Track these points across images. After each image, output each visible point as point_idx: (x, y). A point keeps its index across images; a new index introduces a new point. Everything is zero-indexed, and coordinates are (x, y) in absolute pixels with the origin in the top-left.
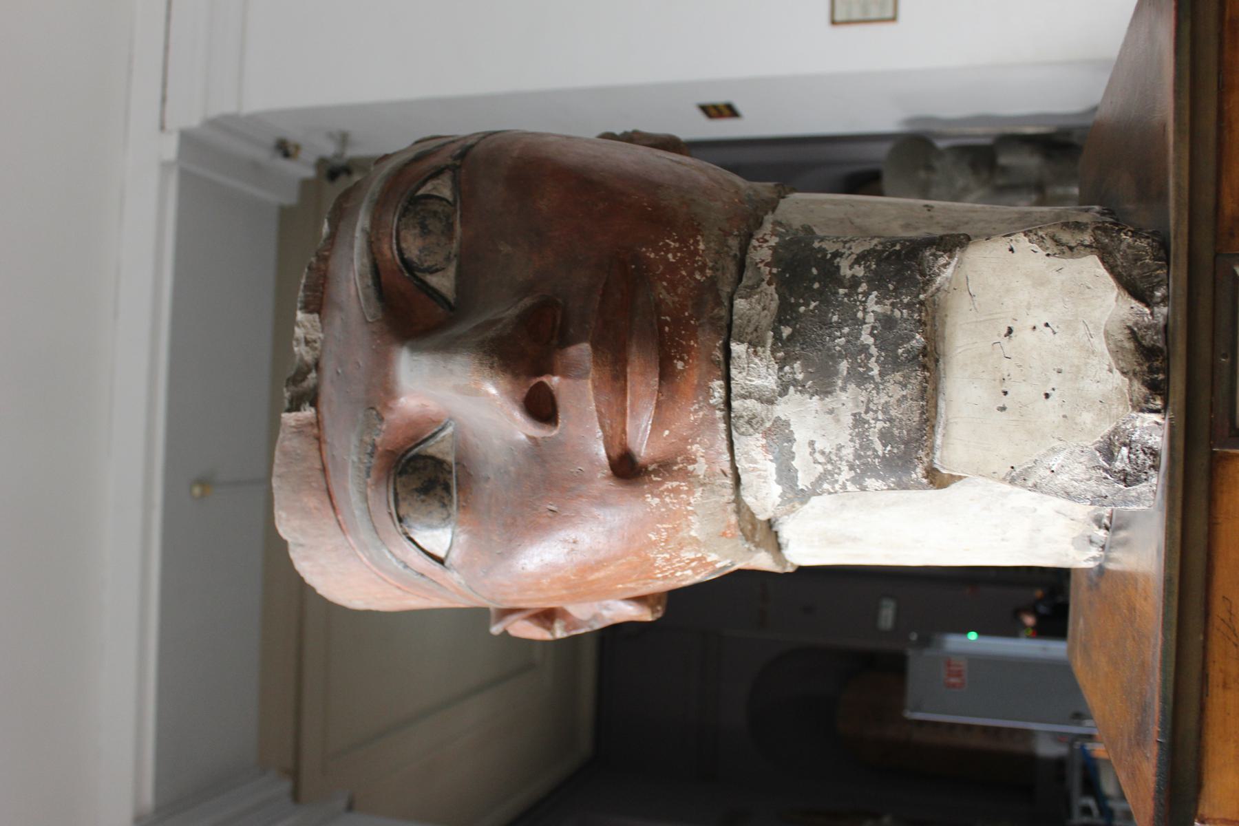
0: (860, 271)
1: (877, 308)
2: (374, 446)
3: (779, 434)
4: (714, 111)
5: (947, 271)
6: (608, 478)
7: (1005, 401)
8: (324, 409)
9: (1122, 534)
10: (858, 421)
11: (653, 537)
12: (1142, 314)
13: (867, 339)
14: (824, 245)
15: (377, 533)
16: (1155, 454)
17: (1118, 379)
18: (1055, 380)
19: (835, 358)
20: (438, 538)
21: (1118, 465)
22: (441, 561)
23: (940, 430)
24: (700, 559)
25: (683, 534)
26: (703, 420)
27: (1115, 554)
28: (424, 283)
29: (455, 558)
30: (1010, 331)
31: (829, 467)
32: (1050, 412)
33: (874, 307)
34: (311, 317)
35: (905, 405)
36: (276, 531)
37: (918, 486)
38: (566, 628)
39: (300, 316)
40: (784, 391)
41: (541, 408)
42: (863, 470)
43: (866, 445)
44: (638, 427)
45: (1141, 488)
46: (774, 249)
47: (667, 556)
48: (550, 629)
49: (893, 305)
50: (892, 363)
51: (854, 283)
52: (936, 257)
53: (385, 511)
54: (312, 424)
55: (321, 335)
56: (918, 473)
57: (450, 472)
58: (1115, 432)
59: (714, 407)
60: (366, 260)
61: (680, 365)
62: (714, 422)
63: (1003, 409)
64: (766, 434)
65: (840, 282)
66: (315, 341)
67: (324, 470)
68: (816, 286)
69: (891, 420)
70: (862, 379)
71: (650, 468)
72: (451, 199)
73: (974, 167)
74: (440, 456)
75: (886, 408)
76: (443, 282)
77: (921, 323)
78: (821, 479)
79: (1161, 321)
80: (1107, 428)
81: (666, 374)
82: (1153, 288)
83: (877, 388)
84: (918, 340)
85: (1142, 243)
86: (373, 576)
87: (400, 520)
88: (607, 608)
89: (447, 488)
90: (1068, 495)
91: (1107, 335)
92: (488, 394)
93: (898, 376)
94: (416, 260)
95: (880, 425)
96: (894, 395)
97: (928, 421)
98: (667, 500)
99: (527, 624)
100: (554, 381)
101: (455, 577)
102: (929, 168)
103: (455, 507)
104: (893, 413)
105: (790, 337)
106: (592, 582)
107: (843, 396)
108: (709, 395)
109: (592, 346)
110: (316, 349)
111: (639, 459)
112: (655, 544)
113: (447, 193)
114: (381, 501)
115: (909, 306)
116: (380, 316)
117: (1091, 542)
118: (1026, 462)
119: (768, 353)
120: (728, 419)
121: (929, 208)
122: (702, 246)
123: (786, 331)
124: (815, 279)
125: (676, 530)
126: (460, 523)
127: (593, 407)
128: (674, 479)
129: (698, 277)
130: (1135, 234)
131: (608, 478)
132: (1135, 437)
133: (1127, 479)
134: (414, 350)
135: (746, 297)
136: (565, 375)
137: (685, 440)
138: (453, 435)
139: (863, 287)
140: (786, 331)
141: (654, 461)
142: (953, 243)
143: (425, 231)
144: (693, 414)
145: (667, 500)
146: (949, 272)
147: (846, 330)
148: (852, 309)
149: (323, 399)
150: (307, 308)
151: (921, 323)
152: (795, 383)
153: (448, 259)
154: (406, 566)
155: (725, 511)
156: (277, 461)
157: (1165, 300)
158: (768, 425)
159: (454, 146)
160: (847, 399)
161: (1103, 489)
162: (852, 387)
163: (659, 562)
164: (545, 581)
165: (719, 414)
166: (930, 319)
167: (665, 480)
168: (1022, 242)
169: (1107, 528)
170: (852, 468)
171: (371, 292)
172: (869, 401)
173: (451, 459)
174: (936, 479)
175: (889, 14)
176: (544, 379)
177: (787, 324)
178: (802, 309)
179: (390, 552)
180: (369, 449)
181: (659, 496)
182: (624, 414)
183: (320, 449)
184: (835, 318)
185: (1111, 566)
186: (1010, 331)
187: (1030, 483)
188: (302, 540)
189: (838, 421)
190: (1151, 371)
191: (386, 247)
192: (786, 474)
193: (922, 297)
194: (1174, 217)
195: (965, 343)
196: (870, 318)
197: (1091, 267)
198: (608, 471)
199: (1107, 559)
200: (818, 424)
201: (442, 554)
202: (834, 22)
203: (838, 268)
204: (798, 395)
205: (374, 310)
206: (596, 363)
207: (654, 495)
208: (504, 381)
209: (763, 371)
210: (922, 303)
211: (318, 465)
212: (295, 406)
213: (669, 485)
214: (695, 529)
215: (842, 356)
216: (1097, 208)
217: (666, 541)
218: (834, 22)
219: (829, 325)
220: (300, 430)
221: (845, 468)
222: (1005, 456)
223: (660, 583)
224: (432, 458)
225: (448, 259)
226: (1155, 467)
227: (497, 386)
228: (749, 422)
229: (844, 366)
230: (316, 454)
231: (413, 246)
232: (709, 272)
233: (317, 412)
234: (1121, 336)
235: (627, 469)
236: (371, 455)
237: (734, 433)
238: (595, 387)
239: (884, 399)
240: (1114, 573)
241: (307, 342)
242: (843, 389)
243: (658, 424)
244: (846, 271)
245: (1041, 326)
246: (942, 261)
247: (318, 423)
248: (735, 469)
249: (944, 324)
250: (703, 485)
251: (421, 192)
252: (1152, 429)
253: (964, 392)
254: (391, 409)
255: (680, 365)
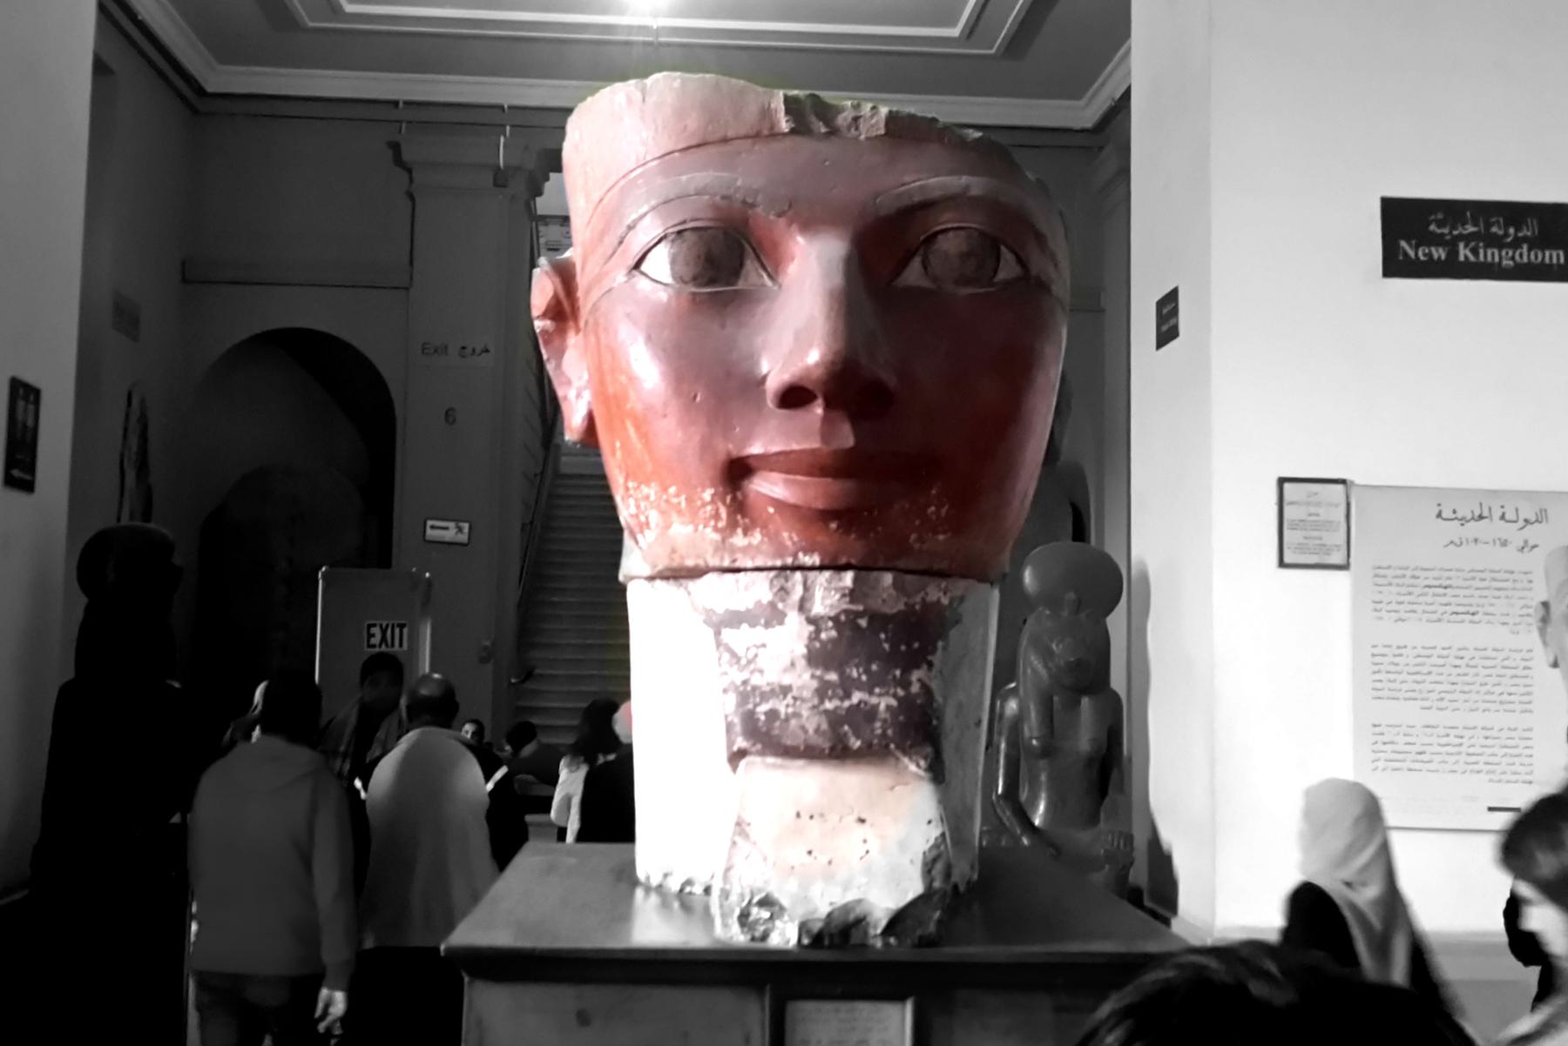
0: (915, 688)
1: (882, 707)
2: (753, 206)
3: (773, 616)
4: (1168, 307)
5: (913, 767)
6: (729, 454)
7: (805, 817)
8: (788, 143)
9: (676, 905)
10: (785, 690)
11: (672, 490)
12: (875, 927)
13: (857, 697)
14: (939, 652)
15: (665, 202)
16: (765, 937)
17: (823, 910)
18: (824, 859)
19: (840, 668)
20: (660, 264)
21: (755, 910)
22: (637, 266)
23: (778, 761)
24: (647, 524)
25: (675, 517)
26: (786, 547)
27: (654, 899)
28: (913, 254)
29: (642, 284)
30: (862, 821)
31: (743, 662)
32: (796, 856)
33: (884, 702)
34: (882, 125)
35: (800, 733)
36: (660, 70)
37: (730, 743)
38: (544, 332)
39: (884, 111)
40: (810, 621)
41: (794, 397)
42: (746, 694)
43: (765, 697)
44: (775, 484)
45: (735, 928)
46: (938, 601)
47: (652, 498)
48: (544, 315)
49: (885, 721)
50: (835, 719)
51: (906, 684)
52: (925, 758)
53: (687, 216)
54: (772, 128)
55: (862, 137)
56: (741, 743)
57: (728, 284)
58: (782, 909)
59: (795, 556)
60: (937, 194)
61: (833, 525)
62: (781, 556)
63: (798, 815)
64: (772, 605)
65: (906, 671)
66: (857, 128)
67: (725, 140)
68: (903, 648)
69: (787, 719)
70: (822, 692)
71: (739, 495)
72: (996, 280)
73: (1077, 667)
74: (744, 272)
75: (797, 715)
76: (913, 275)
77: (870, 745)
78: (734, 654)
79: (871, 942)
80: (785, 902)
81: (825, 515)
82: (897, 937)
83: (814, 707)
84: (856, 744)
85: (932, 928)
86: (614, 179)
87: (679, 233)
88: (579, 396)
89: (711, 282)
90: (728, 870)
91: (859, 901)
92: (806, 354)
93: (825, 726)
94: (936, 247)
95: (782, 710)
96: (809, 723)
97: (789, 752)
98: (709, 508)
99: (550, 293)
100: (818, 410)
101: (621, 277)
102: (1079, 605)
103: (694, 290)
104: (793, 722)
105: (858, 627)
106: (623, 422)
107: (807, 676)
108: (806, 551)
109: (851, 450)
110: (849, 128)
111: (746, 483)
112: (665, 490)
113: (1002, 275)
114: (697, 212)
115: (884, 734)
116: (883, 213)
117: (666, 875)
118: (753, 836)
119: (845, 606)
120: (784, 568)
121: (979, 723)
122: (941, 537)
123: (863, 623)
124: (909, 645)
125: (680, 512)
126: (678, 294)
127: (795, 447)
128: (729, 515)
129: (913, 536)
130: (940, 922)
131: (729, 454)
132: (778, 923)
133: (744, 917)
134: (848, 261)
135: (895, 584)
136: (826, 419)
137: (764, 527)
138: (764, 285)
139: (901, 692)
140: (863, 623)
141: (745, 496)
142: (937, 773)
143: (965, 256)
144: (788, 537)
145: (709, 508)
146: (913, 768)
147: (864, 678)
148: (881, 684)
149: (798, 140)
150: (892, 118)
151: (870, 745)
152: (818, 631)
153: (935, 279)
154: (630, 228)
155: (698, 557)
156: (734, 81)
157: (886, 945)
158: (780, 606)
159: (1051, 269)
160: (804, 680)
161: (734, 898)
162: (815, 684)
163: (645, 490)
164: (623, 378)
165: (789, 561)
166: (874, 753)
167: (728, 507)
168: (935, 832)
169: (681, 891)
170: (745, 683)
171: (906, 202)
172: (803, 700)
173: (741, 285)
174: (736, 757)
175: (1287, 560)
176: (820, 401)
177: (870, 623)
178: (883, 636)
179: (645, 214)
180: (750, 200)
181: (713, 502)
182: (788, 472)
183: (746, 137)
184: (874, 667)
185: (639, 893)
186: (862, 821)
187: (737, 839)
188: (651, 100)
189: (785, 670)
190: (831, 936)
191: (947, 216)
192: (735, 619)
193: (892, 746)
194: (948, 952)
195: (853, 782)
196: (874, 700)
197: (913, 888)
198: (735, 453)
199: (648, 889)
200: (782, 655)
201: (644, 267)
202: (1282, 481)
203: (918, 667)
204: (806, 635)
205: (887, 205)
206: (835, 452)
207: (713, 496)
208: (818, 373)
209: (828, 602)
210: (887, 746)
211: (730, 134)
212: (792, 105)
213: (723, 512)
214: (681, 530)
215: (842, 674)
216: (975, 877)
217: (667, 501)
218: (1282, 481)
219: (869, 661)
220: (766, 113)
221: (745, 675)
222: (748, 802)
223: (621, 480)
224: (741, 265)
225: (935, 279)
226: (753, 939)
227: (817, 365)
228: (782, 589)
229: (833, 677)
230: (742, 132)
231: (950, 245)
232: (917, 546)
233: (784, 135)
234: (859, 911)
235: (737, 472)
236: (744, 202)
237: (772, 574)
238: (813, 451)
239: (805, 713)
240: (631, 895)
241: (856, 119)
242: (813, 676)
243: (778, 504)
244: (915, 675)
245: (867, 847)
246: (922, 763)
247: (774, 135)
248: (738, 570)
249: (869, 763)
250: (723, 540)
251: (1003, 248)
252: (785, 936)
253: (810, 782)
254: (790, 225)
255: (833, 525)
